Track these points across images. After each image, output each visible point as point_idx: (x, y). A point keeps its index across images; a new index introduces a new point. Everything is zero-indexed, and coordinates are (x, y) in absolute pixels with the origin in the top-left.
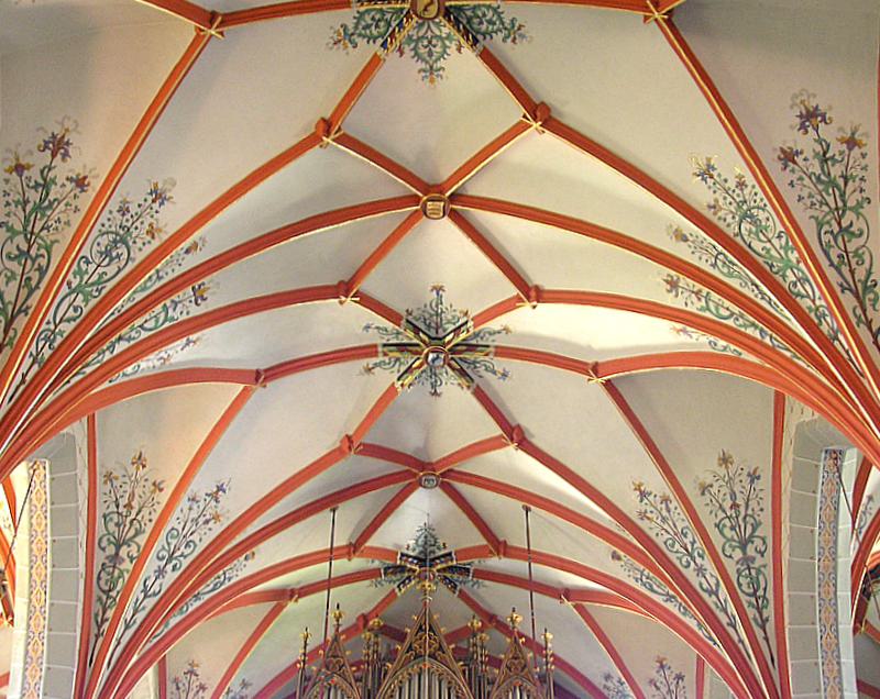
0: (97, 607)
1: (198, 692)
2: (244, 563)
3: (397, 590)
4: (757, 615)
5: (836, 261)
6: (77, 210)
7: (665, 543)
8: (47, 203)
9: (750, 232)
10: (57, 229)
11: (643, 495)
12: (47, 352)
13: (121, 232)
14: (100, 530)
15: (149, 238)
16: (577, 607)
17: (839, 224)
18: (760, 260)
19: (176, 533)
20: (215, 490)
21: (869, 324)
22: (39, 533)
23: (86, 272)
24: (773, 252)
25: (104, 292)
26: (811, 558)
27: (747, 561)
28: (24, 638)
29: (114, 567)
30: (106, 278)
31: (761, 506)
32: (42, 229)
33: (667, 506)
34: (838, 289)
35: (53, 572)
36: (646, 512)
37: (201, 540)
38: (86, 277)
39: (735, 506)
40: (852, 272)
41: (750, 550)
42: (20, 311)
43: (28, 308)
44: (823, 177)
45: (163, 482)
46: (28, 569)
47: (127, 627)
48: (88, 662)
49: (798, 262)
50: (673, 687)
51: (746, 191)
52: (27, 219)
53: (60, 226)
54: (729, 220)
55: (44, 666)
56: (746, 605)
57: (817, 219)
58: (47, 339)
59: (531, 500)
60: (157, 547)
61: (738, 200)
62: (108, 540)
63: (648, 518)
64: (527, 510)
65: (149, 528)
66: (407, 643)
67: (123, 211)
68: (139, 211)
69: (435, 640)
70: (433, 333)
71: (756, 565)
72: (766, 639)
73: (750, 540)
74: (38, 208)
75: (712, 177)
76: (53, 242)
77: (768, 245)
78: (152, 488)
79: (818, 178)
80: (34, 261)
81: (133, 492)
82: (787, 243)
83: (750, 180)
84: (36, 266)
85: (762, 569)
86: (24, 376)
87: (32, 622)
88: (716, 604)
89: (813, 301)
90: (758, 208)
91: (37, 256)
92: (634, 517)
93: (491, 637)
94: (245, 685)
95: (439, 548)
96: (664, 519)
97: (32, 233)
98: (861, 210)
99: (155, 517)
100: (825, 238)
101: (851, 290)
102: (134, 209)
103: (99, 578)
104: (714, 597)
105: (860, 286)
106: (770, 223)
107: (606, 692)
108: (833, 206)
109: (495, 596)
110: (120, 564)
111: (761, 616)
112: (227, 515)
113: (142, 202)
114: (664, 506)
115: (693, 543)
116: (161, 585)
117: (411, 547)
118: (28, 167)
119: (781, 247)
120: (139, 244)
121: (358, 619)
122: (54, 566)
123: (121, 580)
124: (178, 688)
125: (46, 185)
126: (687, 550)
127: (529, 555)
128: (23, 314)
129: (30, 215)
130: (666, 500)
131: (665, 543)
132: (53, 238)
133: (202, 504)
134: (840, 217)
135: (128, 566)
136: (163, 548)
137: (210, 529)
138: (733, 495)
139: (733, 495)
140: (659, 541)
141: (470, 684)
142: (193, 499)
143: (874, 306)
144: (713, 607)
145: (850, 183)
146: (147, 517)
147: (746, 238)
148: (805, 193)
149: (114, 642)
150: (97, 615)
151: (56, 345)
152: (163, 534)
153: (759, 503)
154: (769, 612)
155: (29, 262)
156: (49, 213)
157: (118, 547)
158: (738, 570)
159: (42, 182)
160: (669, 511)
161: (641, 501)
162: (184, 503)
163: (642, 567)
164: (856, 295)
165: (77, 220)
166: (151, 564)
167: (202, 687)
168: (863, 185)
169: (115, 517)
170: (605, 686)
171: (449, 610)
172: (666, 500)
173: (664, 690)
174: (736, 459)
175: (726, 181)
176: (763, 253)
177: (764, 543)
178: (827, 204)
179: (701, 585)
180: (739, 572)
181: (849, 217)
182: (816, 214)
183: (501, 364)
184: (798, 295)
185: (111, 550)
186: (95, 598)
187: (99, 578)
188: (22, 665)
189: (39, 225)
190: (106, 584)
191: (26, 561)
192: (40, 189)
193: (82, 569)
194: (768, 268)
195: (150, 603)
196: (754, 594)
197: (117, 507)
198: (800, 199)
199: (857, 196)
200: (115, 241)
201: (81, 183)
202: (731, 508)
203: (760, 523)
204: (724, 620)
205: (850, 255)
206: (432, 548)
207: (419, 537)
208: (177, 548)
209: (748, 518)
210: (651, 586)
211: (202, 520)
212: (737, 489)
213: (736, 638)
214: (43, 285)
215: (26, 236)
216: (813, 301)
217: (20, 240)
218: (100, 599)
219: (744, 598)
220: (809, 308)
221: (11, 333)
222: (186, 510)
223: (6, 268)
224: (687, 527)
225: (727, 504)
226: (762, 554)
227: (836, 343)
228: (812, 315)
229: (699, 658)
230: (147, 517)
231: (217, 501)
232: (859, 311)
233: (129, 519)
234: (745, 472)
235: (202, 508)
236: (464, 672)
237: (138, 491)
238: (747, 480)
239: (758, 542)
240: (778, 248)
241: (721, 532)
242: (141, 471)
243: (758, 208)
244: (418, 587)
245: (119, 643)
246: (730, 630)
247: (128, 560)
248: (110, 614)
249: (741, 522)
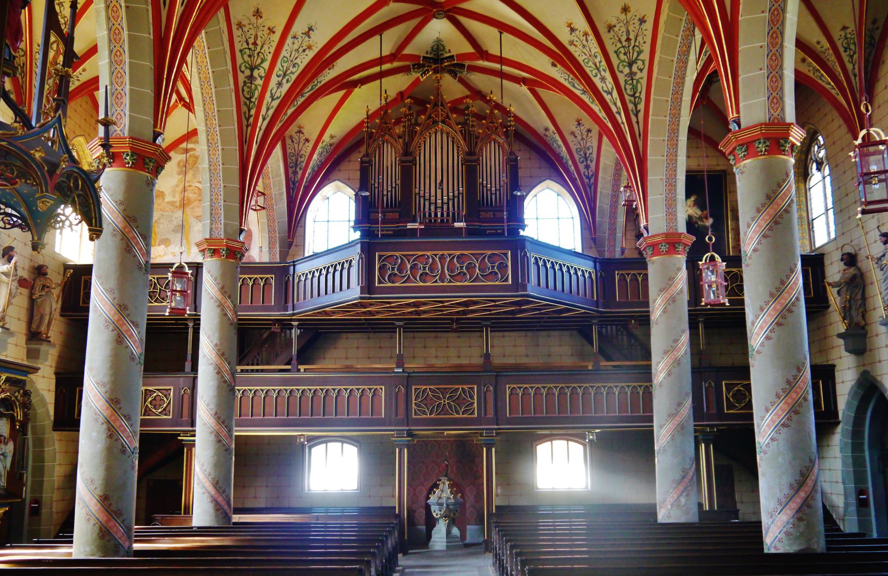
0: (244, 109)
1: (305, 143)
2: (328, 71)
3: (421, 77)
4: (634, 108)
7: (584, 61)
11: (572, 30)
14: (239, 60)
16: (529, 89)
19: (286, 59)
20: (307, 30)
22: (203, 68)
26: (670, 77)
27: (632, 74)
28: (205, 132)
29: (251, 83)
31: (644, 40)
33: (586, 38)
35: (216, 92)
36: (573, 41)
37: (302, 62)
39: (628, 40)
41: (635, 68)
45: (275, 27)
46: (199, 90)
47: (264, 119)
48: (244, 142)
50: (584, 137)
55: (220, 148)
56: (628, 102)
59: (503, 27)
60: (276, 69)
62: (245, 66)
63: (575, 45)
64: (501, 33)
65: (269, 57)
66: (428, 113)
69: (444, 112)
71: (637, 77)
72: (638, 122)
73: (635, 62)
78: (268, 31)
81: (257, 35)
85: (640, 80)
87: (208, 122)
88: (610, 100)
92: (565, 43)
93: (476, 106)
94: (332, 137)
95: (446, 53)
96: (584, 46)
99: (272, 50)
103: (243, 91)
104: (609, 95)
107: (545, 138)
109: (479, 80)
110: (255, 81)
111: (636, 108)
112: (316, 45)
114: (584, 38)
115: (600, 62)
116: (281, 92)
117: (429, 52)
121: (397, 95)
122: (216, 87)
123: (256, 91)
124: (293, 142)
126: (596, 66)
127: (501, 60)
130: (586, 34)
131: (584, 61)
133: (300, 40)
135: (259, 82)
136: (280, 70)
137: (307, 55)
138: (628, 32)
139: (628, 32)
140: (580, 59)
141: (465, 141)
142: (295, 37)
144: (609, 101)
146: (267, 51)
149: (258, 129)
150: (245, 113)
152: (279, 61)
153: (643, 38)
154: (641, 107)
157: (252, 69)
158: (626, 80)
160: (587, 41)
161: (571, 34)
162: (289, 40)
163: (569, 73)
166: (274, 80)
167: (307, 140)
169: (247, 51)
170: (545, 135)
171: (451, 88)
172: (586, 34)
173: (579, 138)
174: (632, 9)
177: (644, 64)
179: (603, 88)
180: (626, 82)
185: (248, 73)
186: (242, 103)
187: (243, 91)
188: (206, 148)
190: (248, 94)
191: (198, 84)
193: (232, 86)
195: (276, 103)
196: (633, 95)
197: (248, 44)
202: (626, 41)
203: (643, 51)
204: (614, 109)
206: (442, 52)
207: (433, 46)
208: (288, 69)
209: (635, 48)
210: (574, 84)
211: (301, 50)
212: (631, 28)
213: (620, 121)
218: (245, 104)
219: (627, 98)
222: (291, 45)
224: (597, 52)
225: (624, 38)
226: (641, 70)
229: (600, 131)
230: (267, 51)
231: (309, 38)
233: (256, 53)
234: (637, 18)
235: (300, 42)
236: (461, 131)
237: (260, 34)
238: (637, 23)
239: (640, 63)
241: (618, 56)
242: (260, 21)
244: (434, 77)
245: (260, 129)
246: (617, 116)
247: (259, 79)
248: (253, 112)
249: (631, 51)
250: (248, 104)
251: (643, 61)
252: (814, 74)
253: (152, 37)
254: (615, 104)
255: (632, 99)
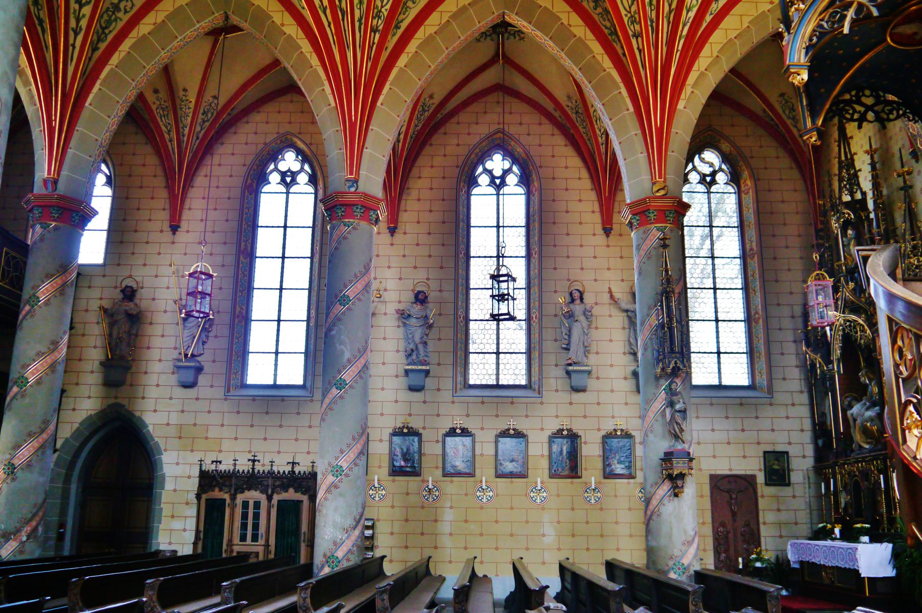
4: (95, 42)
88: (75, 11)
89: (382, 7)
111: (97, 43)
154: (103, 46)
158: (108, 8)
177: (131, 8)
196: (103, 29)
204: (73, 23)
216: (382, 7)
250: (876, 108)
251: (133, 5)
252: (157, 109)
254: (78, 20)
255: (100, 31)
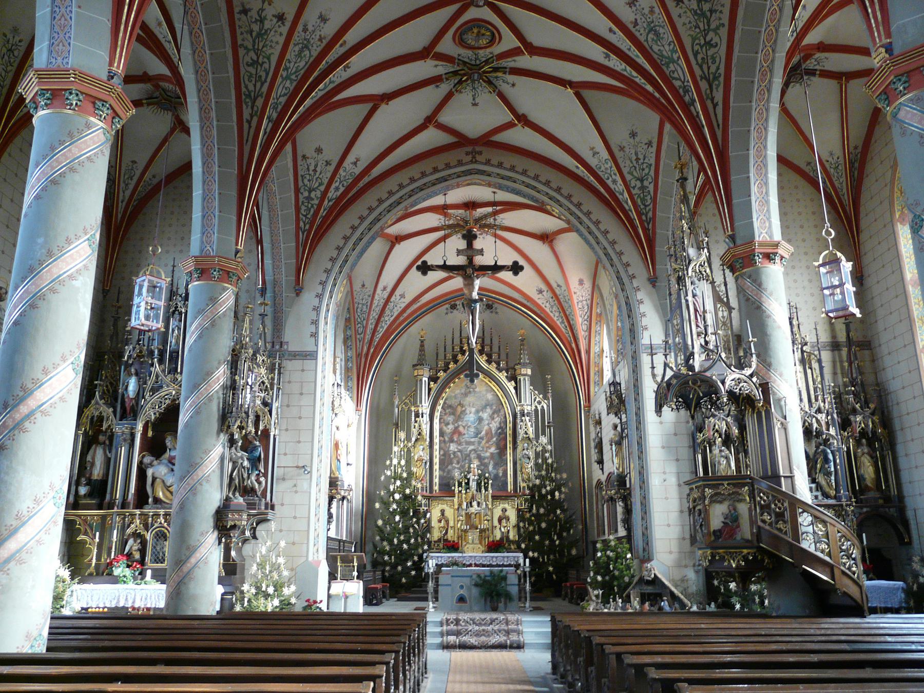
5: (700, 61)
6: (281, 34)
8: (263, 31)
9: (653, 39)
10: (271, 46)
12: (275, 115)
13: (305, 42)
15: (319, 43)
17: (705, 39)
18: (655, 56)
21: (712, 99)
23: (290, 67)
24: (664, 53)
25: (299, 77)
27: (643, 188)
30: (300, 68)
32: (263, 47)
34: (699, 79)
38: (290, 70)
39: (637, 159)
40: (709, 68)
42: (258, 96)
43: (262, 93)
44: (698, 11)
49: (679, 58)
51: (654, 16)
52: (254, 41)
53: (273, 45)
54: (642, 31)
57: (691, 36)
58: (275, 108)
61: (649, 20)
67: (305, 30)
68: (313, 29)
70: (473, 62)
74: (259, 35)
75: (635, 6)
76: (270, 55)
77: (662, 48)
79: (695, 12)
80: (261, 66)
82: (673, 48)
83: (656, 10)
84: (263, 69)
86: (265, 130)
89: (683, 83)
90: (660, 26)
91: (263, 63)
97: (258, 50)
98: (718, 31)
100: (696, 48)
101: (705, 78)
102: (310, 28)
105: (711, 76)
106: (666, 36)
108: (702, 29)
113: (314, 24)
118: (250, 10)
119: (669, 50)
120: (314, 45)
125: (262, 21)
128: (260, 98)
129: (255, 39)
132: (270, 51)
134: (706, 35)
143: (717, 88)
145: (714, 15)
147: (650, 43)
148: (687, 22)
151: (279, 110)
155: (259, 67)
156: (265, 37)
159: (258, 18)
164: (708, 81)
165: (282, 40)
168: (721, 16)
175: (643, 9)
176: (658, 53)
178: (700, 29)
181: (711, 35)
182: (692, 33)
183: (511, 78)
184: (674, 78)
189: (261, 44)
192: (259, 23)
194: (659, 61)
198: (684, 24)
199: (717, 23)
200: (303, 48)
201: (281, 18)
205: (709, 58)
214: (269, 80)
215: (255, 51)
216: (683, 83)
217: (252, 54)
220: (680, 87)
221: (255, 108)
223: (247, 71)
225: (635, 157)
227: (692, 108)
228: (681, 91)
232: (708, 91)
240: (667, 49)
243: (660, 26)
253: (236, 172)
